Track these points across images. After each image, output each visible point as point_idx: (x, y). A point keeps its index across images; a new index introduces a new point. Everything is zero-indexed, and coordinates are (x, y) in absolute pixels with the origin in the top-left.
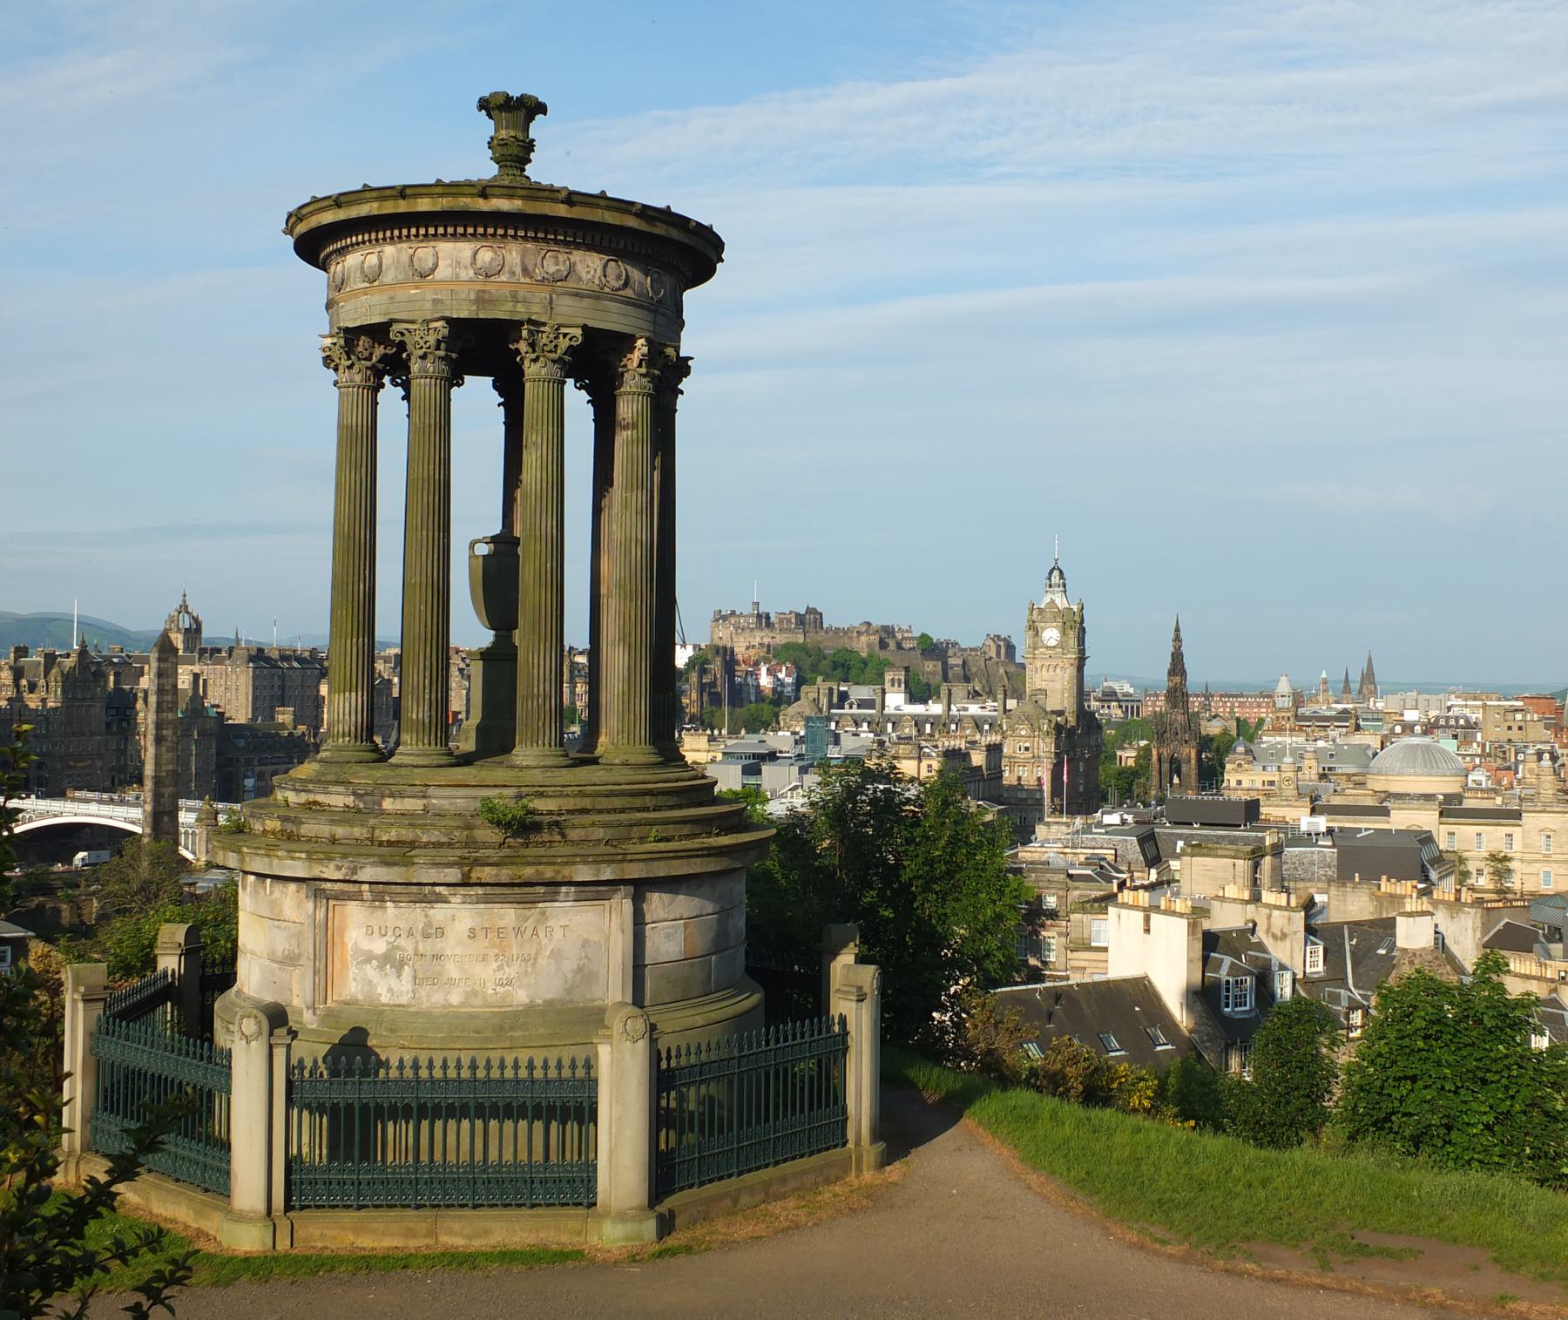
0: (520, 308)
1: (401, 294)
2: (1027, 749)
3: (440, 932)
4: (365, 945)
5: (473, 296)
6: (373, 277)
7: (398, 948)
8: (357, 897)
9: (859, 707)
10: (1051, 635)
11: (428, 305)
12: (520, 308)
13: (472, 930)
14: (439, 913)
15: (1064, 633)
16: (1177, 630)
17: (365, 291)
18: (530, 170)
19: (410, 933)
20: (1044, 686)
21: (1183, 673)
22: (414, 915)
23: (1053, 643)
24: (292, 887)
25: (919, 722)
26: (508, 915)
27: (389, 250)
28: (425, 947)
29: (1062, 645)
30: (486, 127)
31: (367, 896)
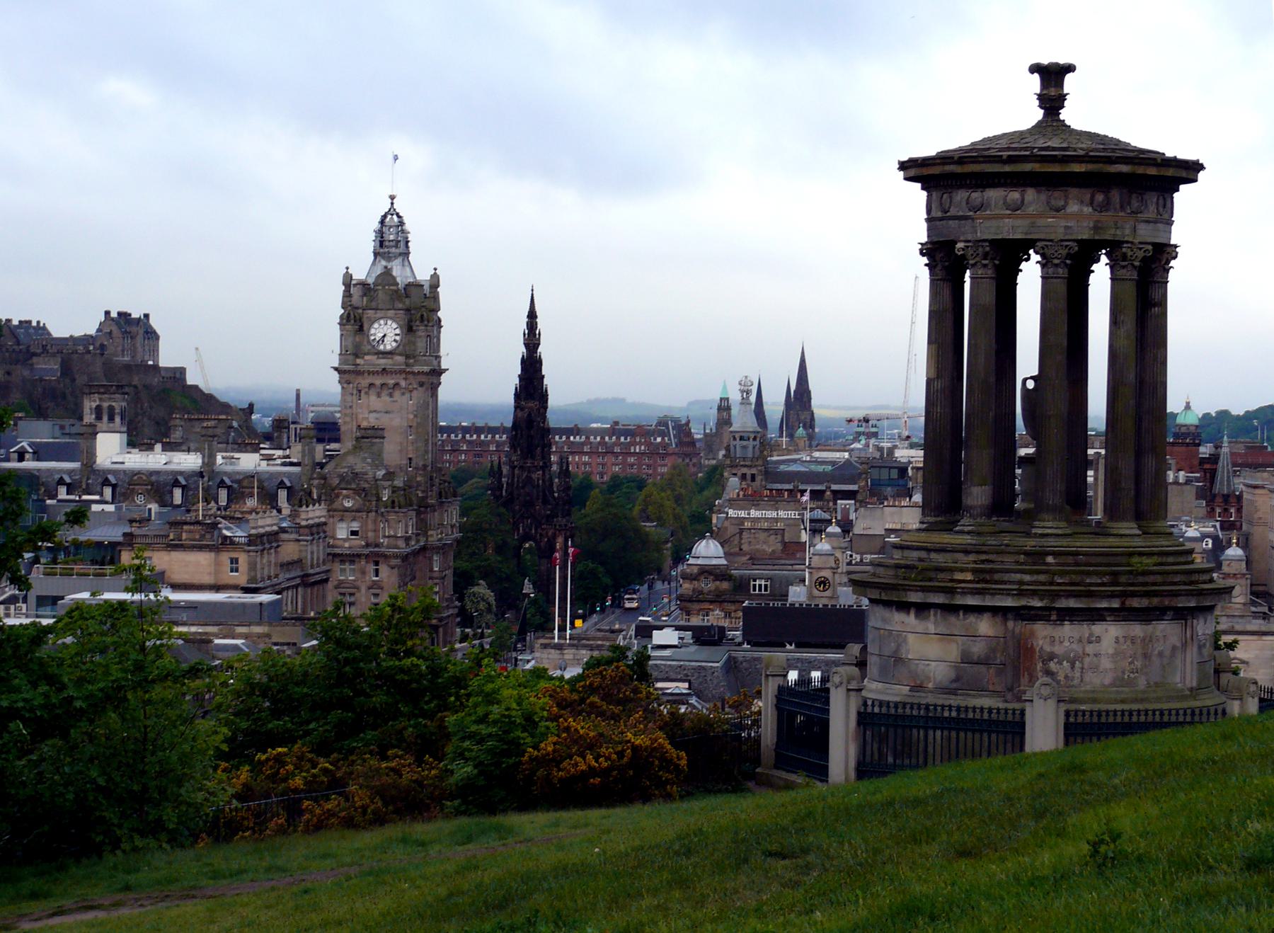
0: (1118, 232)
1: (1041, 222)
2: (354, 533)
3: (1098, 640)
4: (1048, 648)
5: (1091, 225)
6: (1016, 207)
7: (1073, 650)
8: (1046, 619)
9: (38, 456)
10: (386, 332)
11: (1062, 230)
12: (1118, 232)
13: (1117, 638)
14: (1098, 628)
15: (409, 329)
16: (532, 315)
17: (1009, 216)
18: (1065, 115)
19: (1080, 641)
20: (372, 420)
21: (543, 397)
22: (1083, 629)
23: (389, 345)
24: (987, 616)
25: (158, 486)
26: (1137, 629)
27: (1030, 194)
28: (1090, 649)
29: (406, 350)
30: (1034, 83)
31: (1054, 617)
